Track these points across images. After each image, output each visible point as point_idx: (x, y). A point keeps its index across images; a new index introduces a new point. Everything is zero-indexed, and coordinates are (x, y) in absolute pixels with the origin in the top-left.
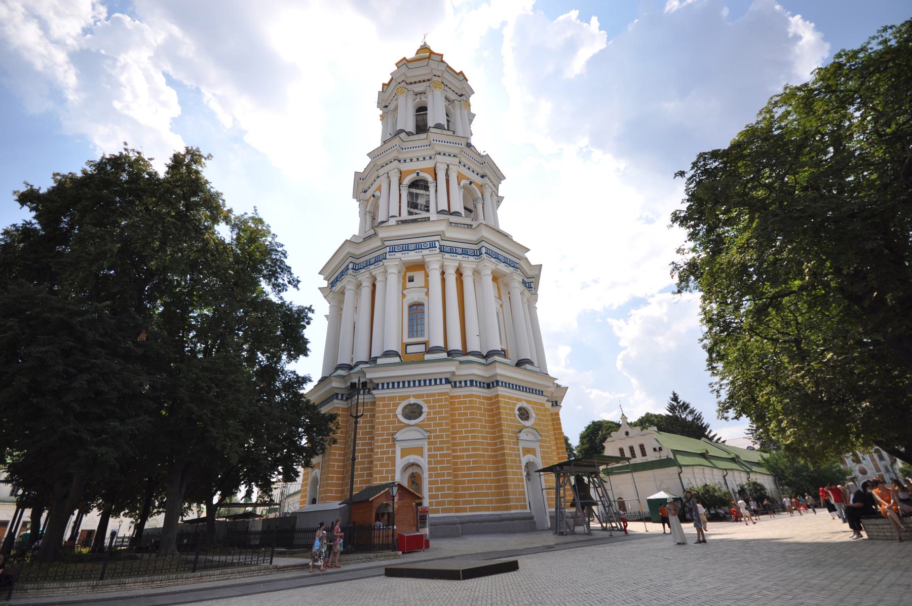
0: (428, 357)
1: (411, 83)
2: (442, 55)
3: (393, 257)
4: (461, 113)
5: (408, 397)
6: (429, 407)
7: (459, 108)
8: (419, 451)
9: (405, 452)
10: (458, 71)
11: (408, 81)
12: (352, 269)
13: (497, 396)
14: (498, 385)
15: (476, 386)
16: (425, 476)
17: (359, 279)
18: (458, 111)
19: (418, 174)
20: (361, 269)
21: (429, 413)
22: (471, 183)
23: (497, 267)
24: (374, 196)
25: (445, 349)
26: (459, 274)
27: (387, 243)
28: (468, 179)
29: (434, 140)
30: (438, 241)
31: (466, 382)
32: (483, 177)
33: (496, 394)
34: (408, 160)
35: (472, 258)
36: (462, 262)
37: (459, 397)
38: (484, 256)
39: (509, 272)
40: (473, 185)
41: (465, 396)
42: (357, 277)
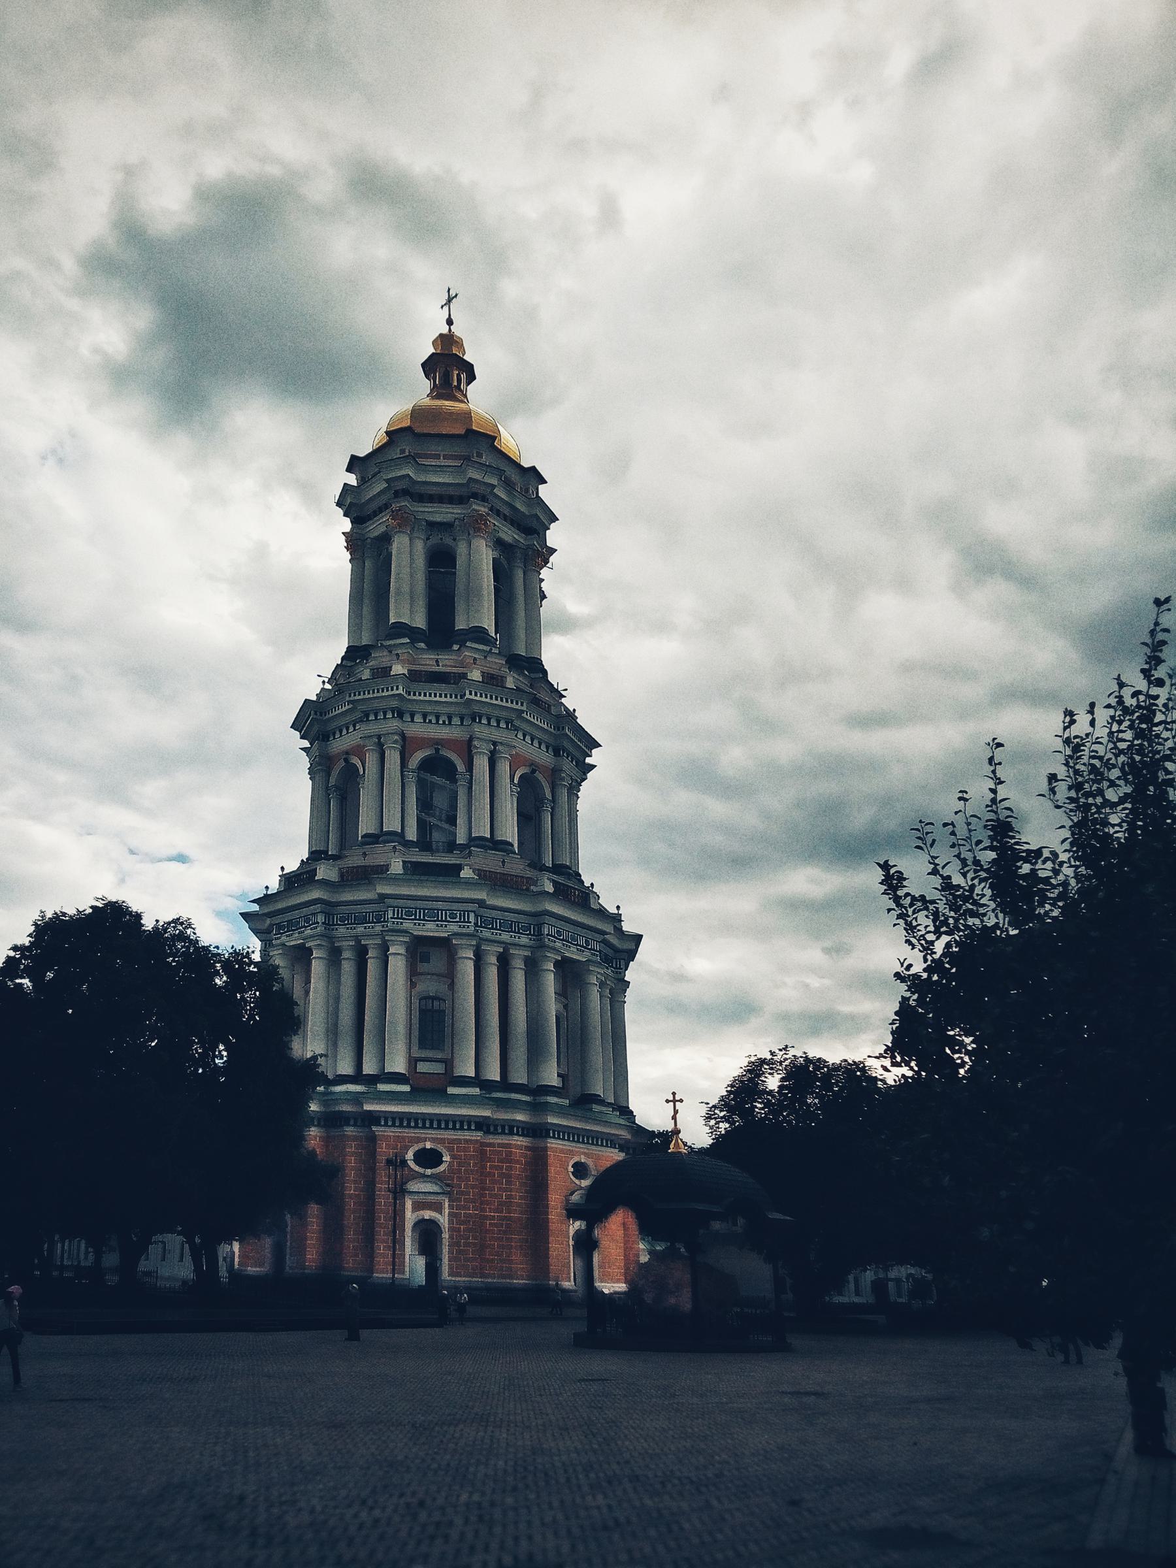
0: (451, 1090)
5: (425, 1140)
6: (453, 1157)
8: (438, 1208)
9: (417, 1206)
10: (526, 464)
13: (545, 1149)
14: (548, 1136)
15: (517, 1134)
16: (446, 1235)
18: (519, 574)
21: (451, 1164)
22: (533, 771)
25: (478, 1081)
26: (504, 963)
29: (471, 694)
30: (474, 912)
31: (503, 1127)
32: (557, 752)
33: (542, 1145)
37: (490, 1145)
41: (500, 1145)
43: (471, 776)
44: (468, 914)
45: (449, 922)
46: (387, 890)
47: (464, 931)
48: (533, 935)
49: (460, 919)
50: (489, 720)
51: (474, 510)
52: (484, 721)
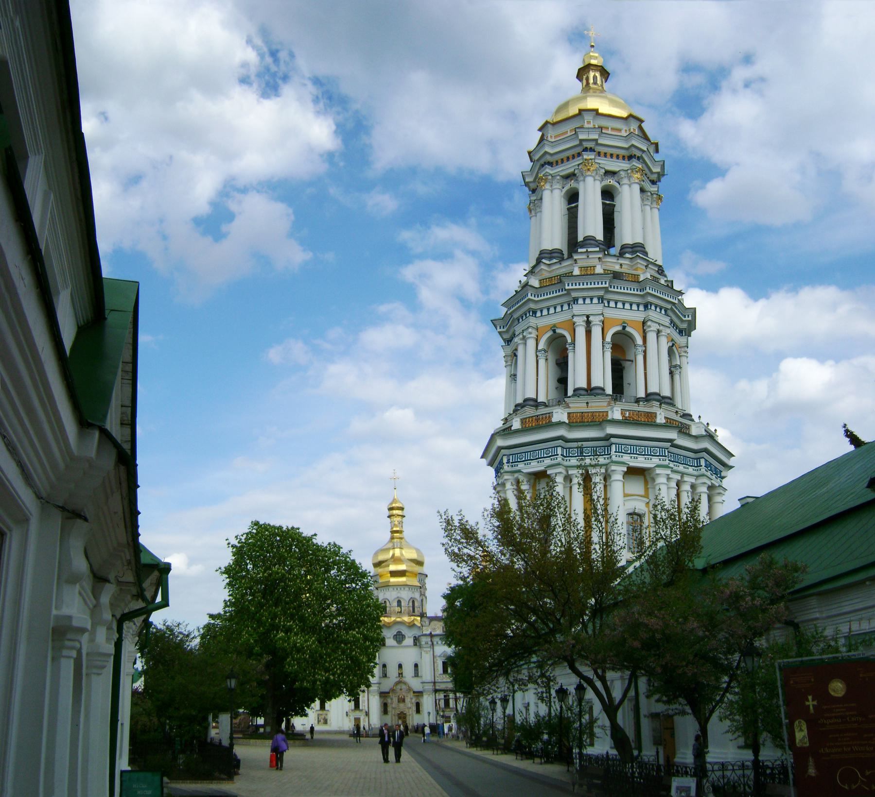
1: (599, 154)
2: (642, 121)
3: (617, 459)
4: (651, 209)
7: (649, 204)
11: (598, 149)
12: (561, 455)
17: (570, 472)
19: (624, 328)
20: (571, 457)
23: (712, 481)
24: (554, 331)
27: (613, 440)
28: (672, 340)
30: (667, 449)
34: (612, 304)
35: (690, 470)
36: (685, 475)
38: (703, 470)
39: (717, 485)
40: (674, 348)
42: (568, 469)
43: (645, 347)
44: (665, 450)
45: (653, 456)
46: (611, 430)
47: (662, 463)
48: (694, 466)
49: (660, 453)
50: (656, 308)
51: (634, 165)
52: (653, 307)
